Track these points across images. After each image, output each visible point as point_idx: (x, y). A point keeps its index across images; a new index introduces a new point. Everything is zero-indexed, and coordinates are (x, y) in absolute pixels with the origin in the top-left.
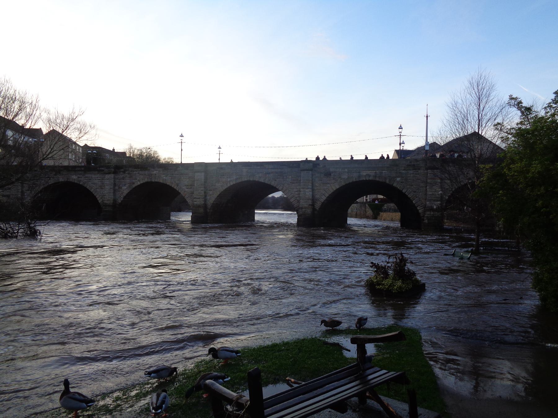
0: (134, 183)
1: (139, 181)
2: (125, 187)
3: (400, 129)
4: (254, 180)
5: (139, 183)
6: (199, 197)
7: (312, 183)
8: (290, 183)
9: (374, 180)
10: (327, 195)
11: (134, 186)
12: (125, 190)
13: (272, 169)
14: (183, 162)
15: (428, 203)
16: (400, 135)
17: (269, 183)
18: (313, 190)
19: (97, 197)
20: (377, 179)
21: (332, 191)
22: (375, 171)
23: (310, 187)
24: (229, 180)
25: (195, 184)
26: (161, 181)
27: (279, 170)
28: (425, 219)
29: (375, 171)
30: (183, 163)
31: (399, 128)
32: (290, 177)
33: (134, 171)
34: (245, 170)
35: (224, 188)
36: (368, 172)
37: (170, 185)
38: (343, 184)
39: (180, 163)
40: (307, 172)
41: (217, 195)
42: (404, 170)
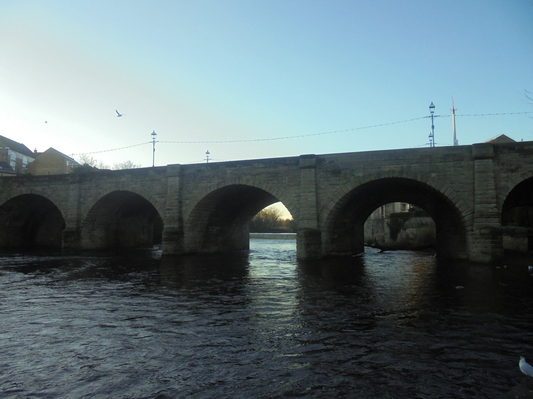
1: (106, 190)
4: (240, 183)
5: (105, 193)
8: (288, 185)
9: (400, 177)
11: (100, 197)
13: (263, 168)
15: (478, 206)
17: (259, 187)
18: (317, 194)
19: (61, 211)
20: (405, 176)
22: (400, 166)
23: (313, 190)
24: (209, 185)
26: (130, 190)
27: (272, 170)
28: (474, 229)
29: (400, 166)
30: (155, 166)
31: (430, 107)
34: (229, 171)
37: (140, 194)
38: (357, 184)
39: (152, 166)
40: (309, 170)
41: (195, 205)
42: (441, 162)
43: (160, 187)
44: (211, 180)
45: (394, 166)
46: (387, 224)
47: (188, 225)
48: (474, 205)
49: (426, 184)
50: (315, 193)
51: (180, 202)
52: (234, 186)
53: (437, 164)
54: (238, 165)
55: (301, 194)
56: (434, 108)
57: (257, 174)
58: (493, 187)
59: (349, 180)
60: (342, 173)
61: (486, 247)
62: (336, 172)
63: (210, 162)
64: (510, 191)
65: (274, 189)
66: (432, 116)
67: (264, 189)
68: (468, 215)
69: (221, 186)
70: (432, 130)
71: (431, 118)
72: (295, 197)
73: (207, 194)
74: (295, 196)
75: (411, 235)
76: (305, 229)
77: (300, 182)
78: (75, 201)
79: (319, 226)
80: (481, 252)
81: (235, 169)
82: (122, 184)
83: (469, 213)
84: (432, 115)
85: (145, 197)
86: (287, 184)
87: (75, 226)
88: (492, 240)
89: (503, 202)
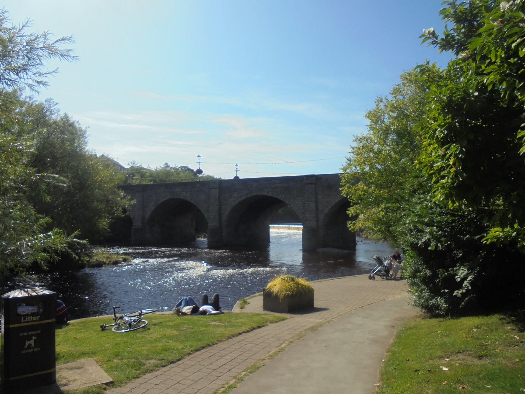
5: (163, 200)
10: (330, 207)
17: (276, 197)
26: (182, 197)
67: (280, 199)
69: (249, 196)
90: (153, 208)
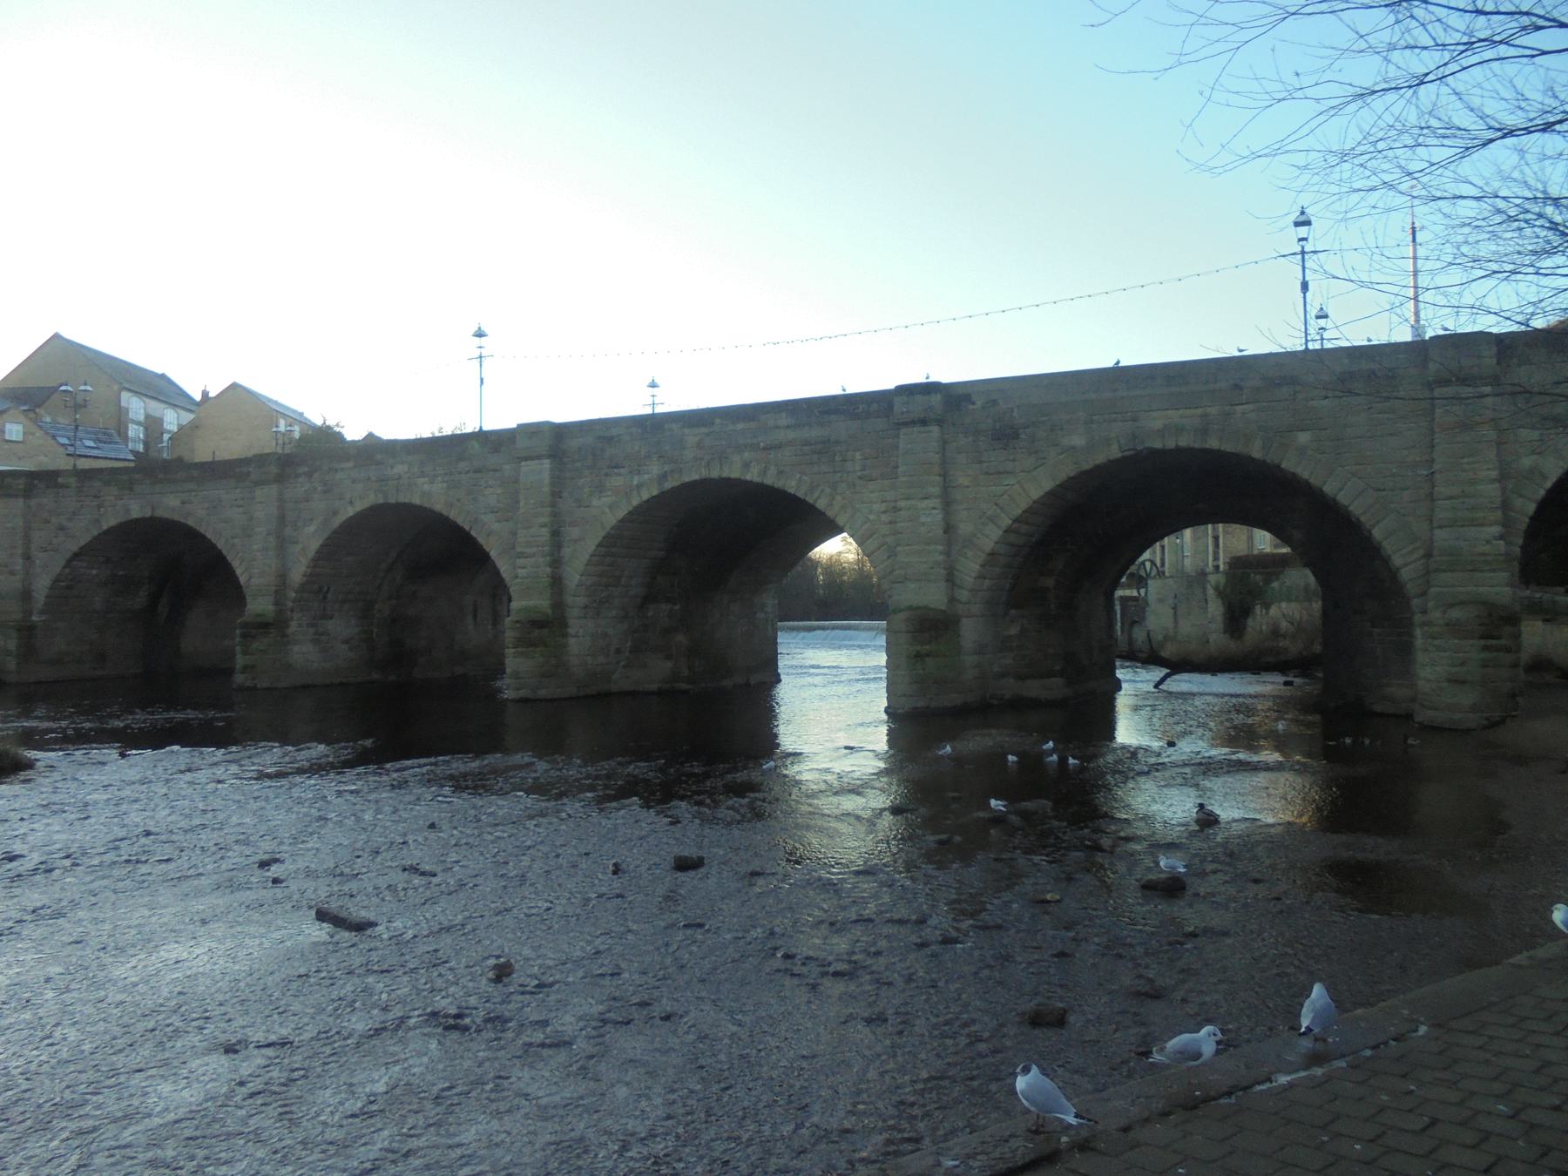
0: (335, 513)
1: (351, 503)
2: (312, 528)
3: (1319, 321)
5: (351, 512)
6: (535, 549)
7: (944, 476)
8: (860, 478)
9: (1197, 446)
11: (337, 521)
12: (310, 539)
13: (788, 427)
14: (485, 429)
15: (1440, 534)
16: (1303, 253)
17: (779, 484)
18: (947, 504)
20: (1213, 443)
21: (1023, 504)
22: (1199, 411)
23: (936, 490)
25: (522, 504)
26: (417, 501)
27: (815, 433)
29: (1199, 411)
31: (1297, 224)
32: (858, 456)
33: (336, 470)
35: (622, 512)
36: (1174, 416)
37: (445, 513)
38: (1067, 470)
40: (922, 429)
43: (499, 492)
44: (639, 466)
45: (1181, 412)
46: (1216, 588)
47: (581, 601)
48: (1432, 529)
49: (1278, 466)
50: (939, 500)
51: (556, 534)
52: (704, 483)
53: (1314, 403)
54: (718, 421)
55: (902, 504)
56: (1307, 227)
57: (770, 449)
58: (1494, 474)
59: (1045, 458)
60: (1023, 436)
61: (1463, 664)
62: (1006, 435)
63: (659, 410)
64: (1549, 484)
65: (822, 491)
66: (1303, 253)
67: (792, 491)
68: (1410, 564)
69: (668, 485)
70: (1302, 295)
71: (1299, 257)
72: (884, 512)
73: (631, 509)
74: (883, 509)
75: (1284, 624)
76: (910, 608)
77: (897, 467)
78: (268, 534)
79: (952, 600)
80: (1449, 681)
81: (708, 435)
82: (395, 482)
83: (1415, 556)
84: (1303, 247)
85: (460, 521)
86: (859, 474)
87: (271, 608)
88: (1483, 642)
89: (1527, 520)
90: (315, 545)
